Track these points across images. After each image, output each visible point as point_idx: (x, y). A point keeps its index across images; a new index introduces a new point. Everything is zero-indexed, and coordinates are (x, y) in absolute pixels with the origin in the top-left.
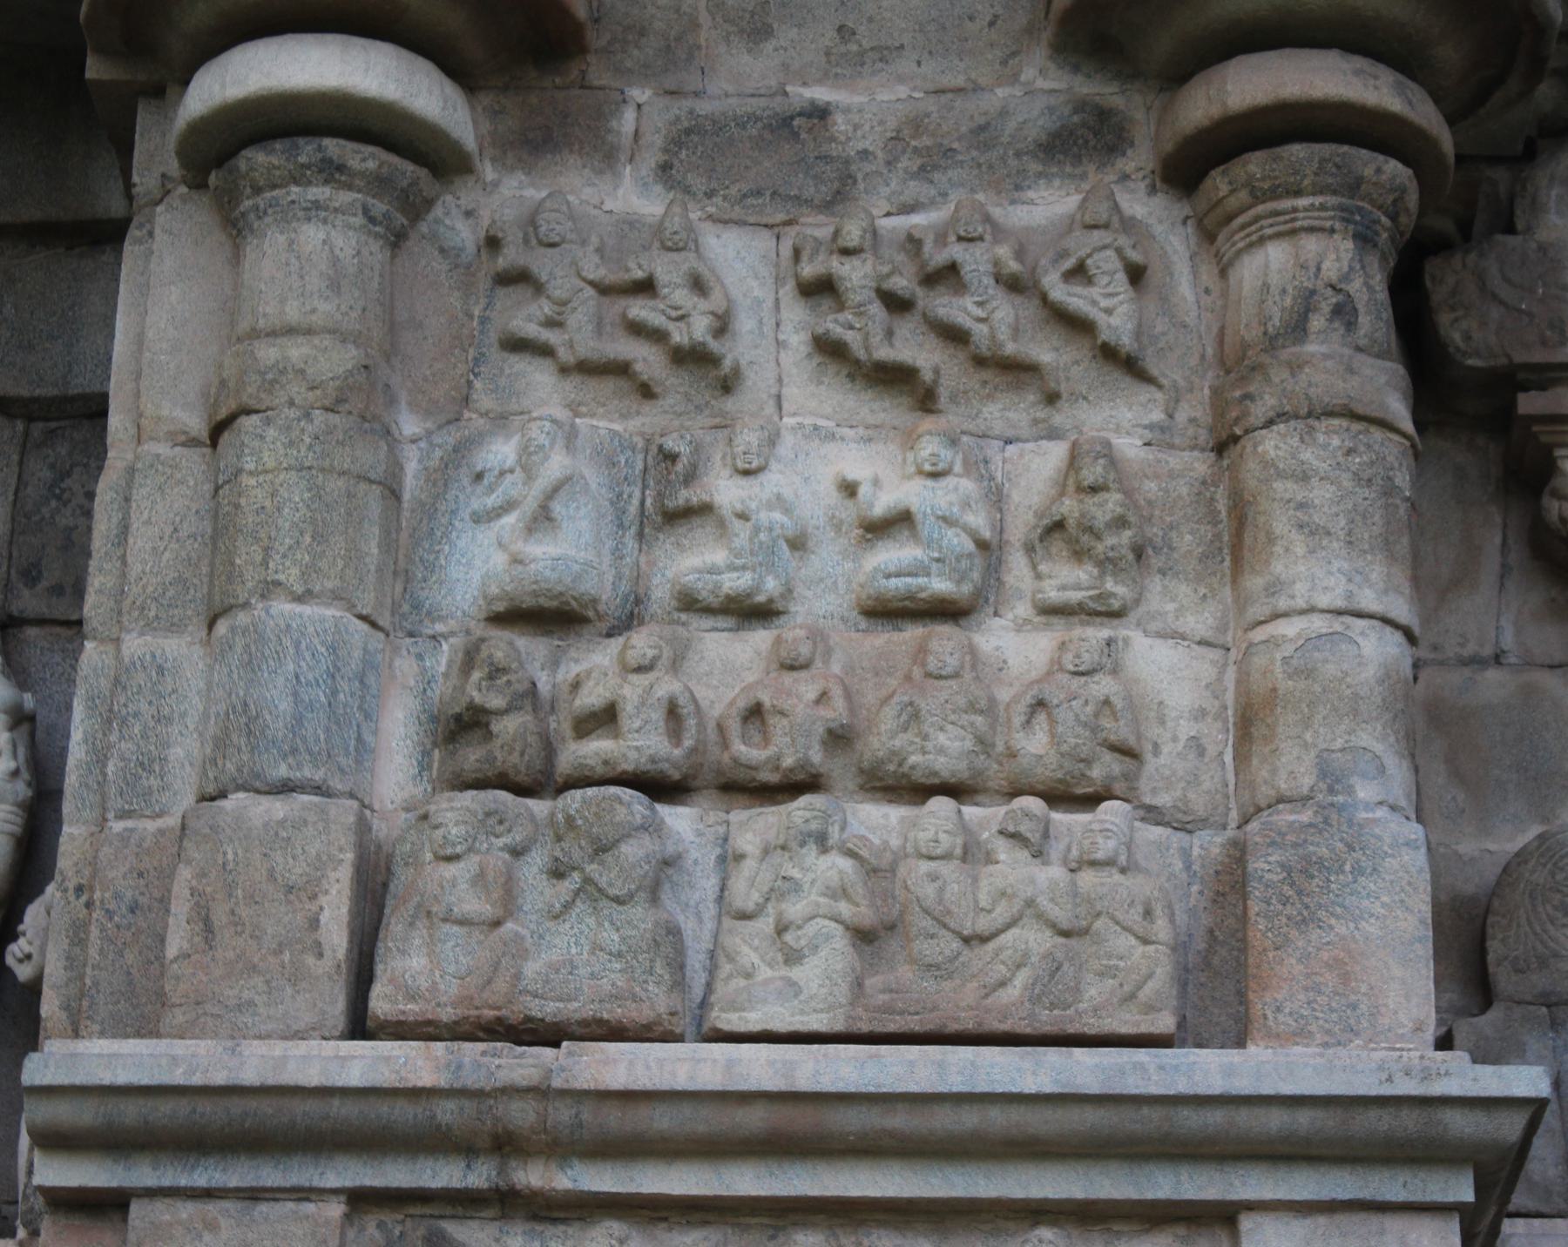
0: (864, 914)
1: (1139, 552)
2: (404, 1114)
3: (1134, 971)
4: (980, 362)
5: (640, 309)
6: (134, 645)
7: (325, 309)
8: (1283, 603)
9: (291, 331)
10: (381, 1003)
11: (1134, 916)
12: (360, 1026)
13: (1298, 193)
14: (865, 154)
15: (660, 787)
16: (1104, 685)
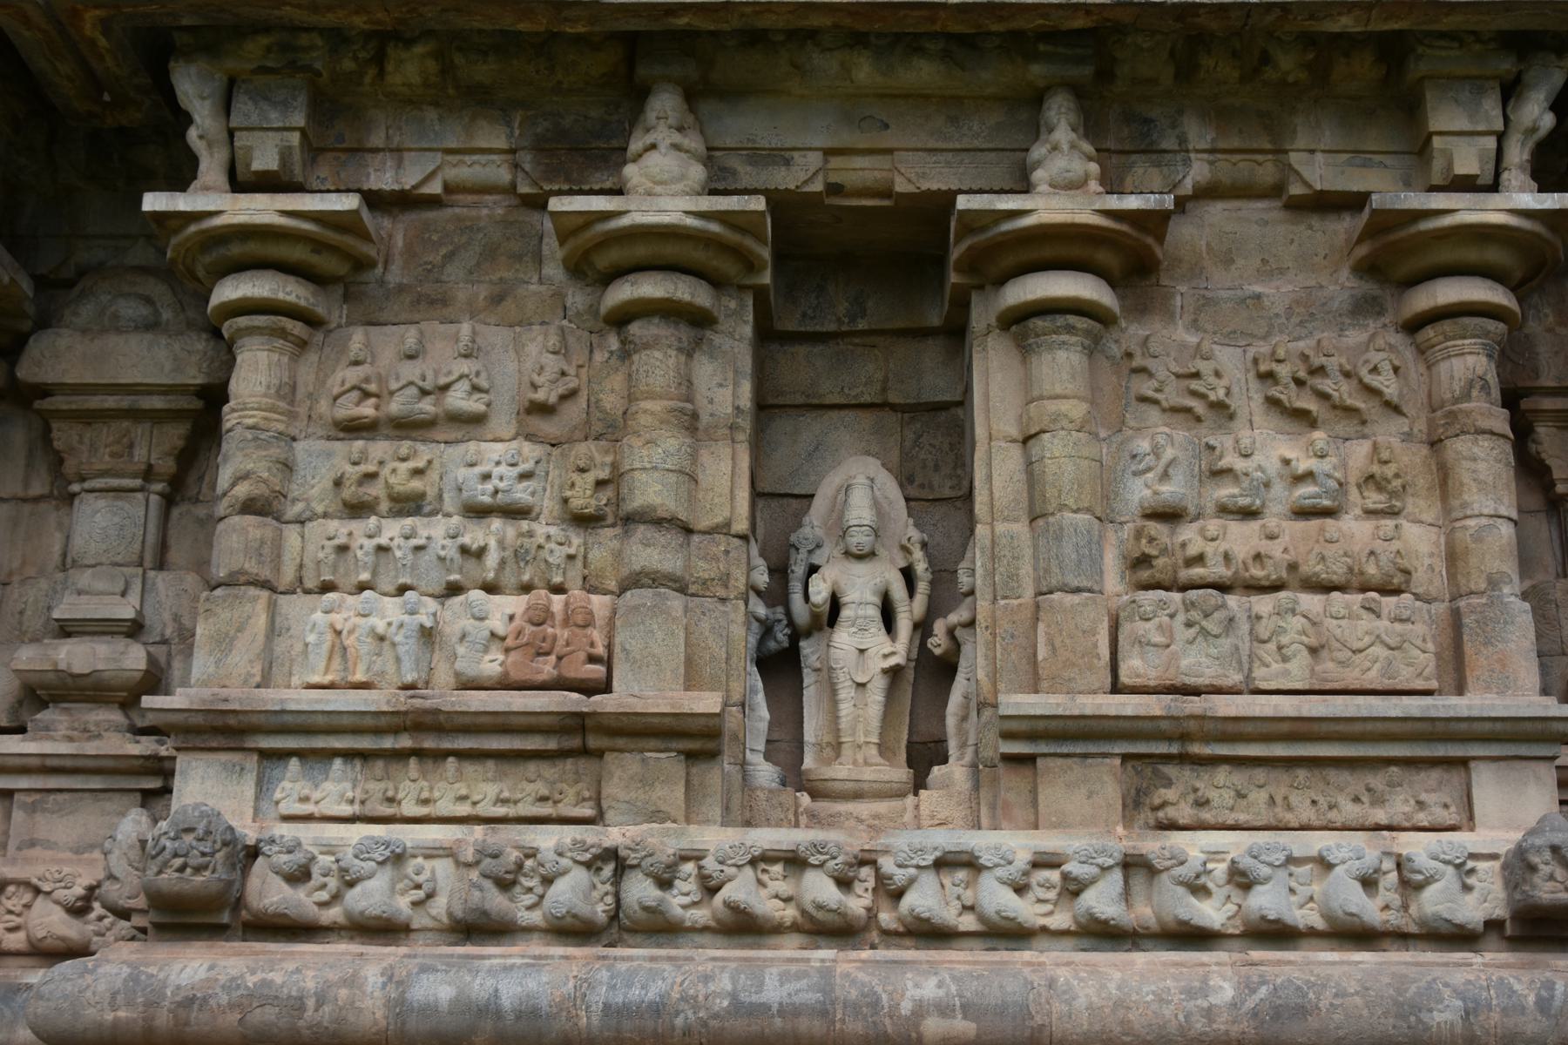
0: (1313, 641)
1: (1404, 487)
2: (1148, 725)
3: (1419, 665)
4: (1335, 407)
5: (1195, 385)
6: (1001, 528)
7: (1070, 388)
8: (1469, 512)
9: (1057, 397)
10: (1125, 678)
11: (1419, 642)
12: (1116, 688)
13: (1465, 338)
14: (1277, 315)
15: (1223, 588)
16: (1396, 545)
